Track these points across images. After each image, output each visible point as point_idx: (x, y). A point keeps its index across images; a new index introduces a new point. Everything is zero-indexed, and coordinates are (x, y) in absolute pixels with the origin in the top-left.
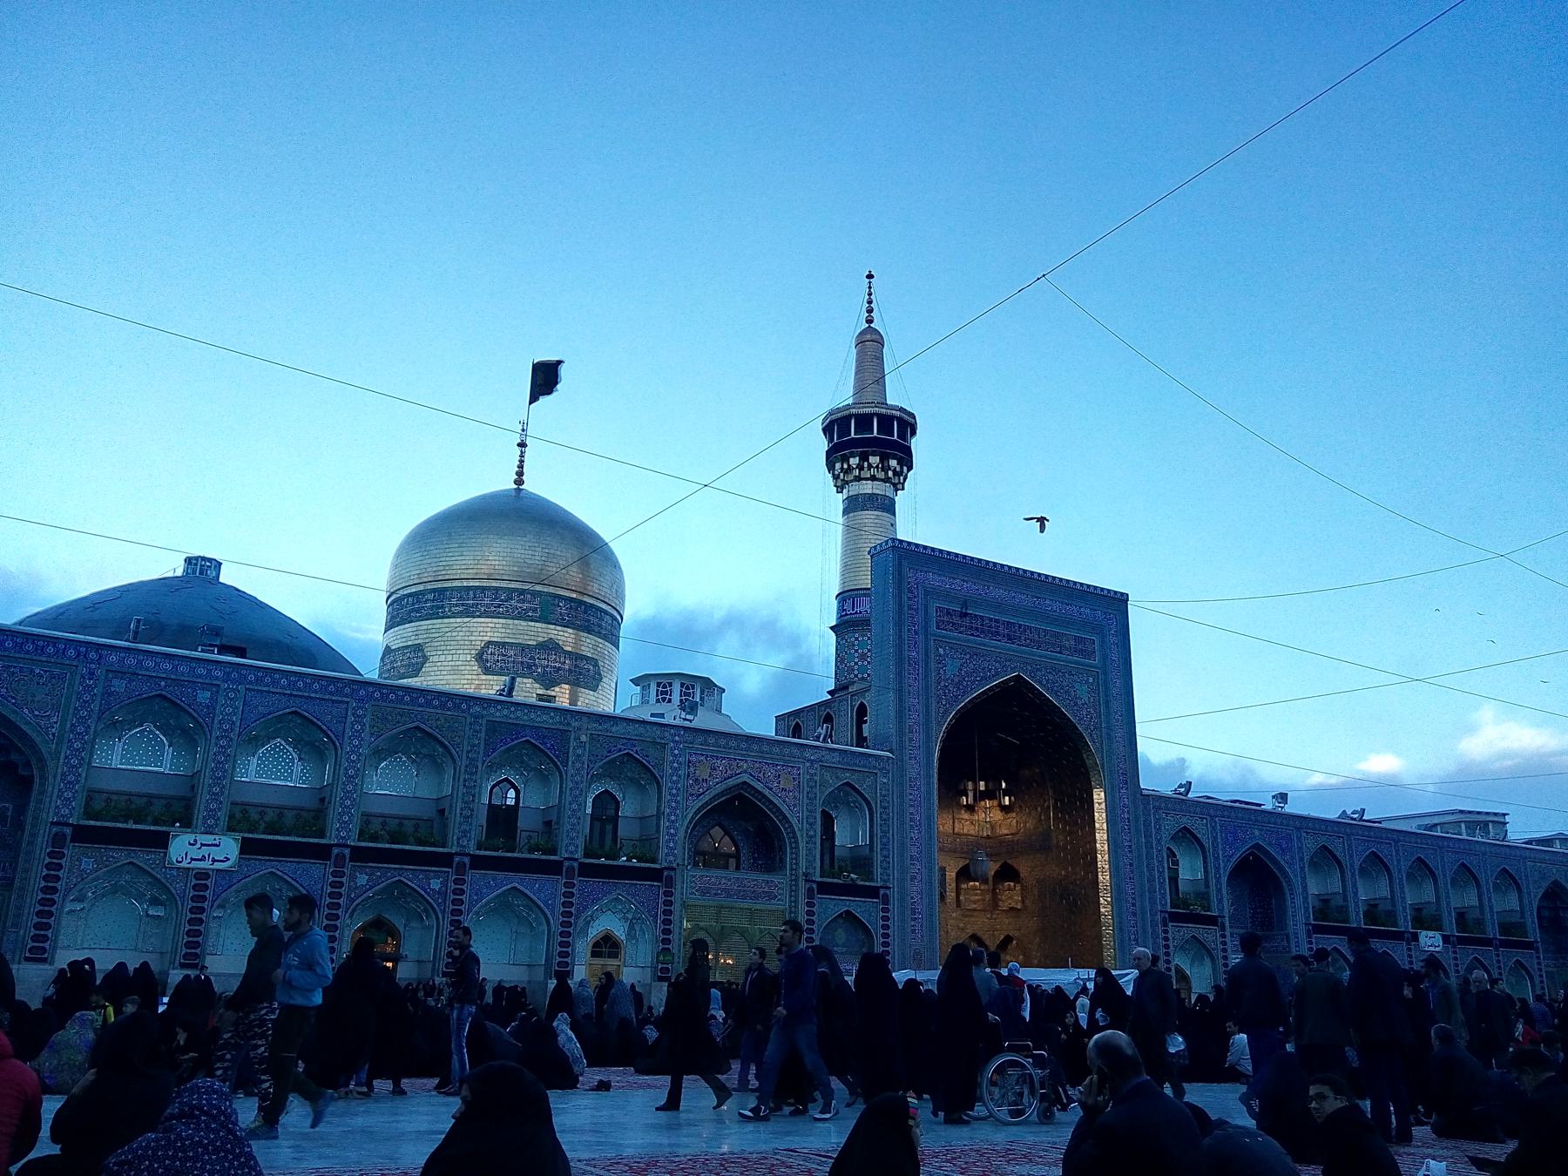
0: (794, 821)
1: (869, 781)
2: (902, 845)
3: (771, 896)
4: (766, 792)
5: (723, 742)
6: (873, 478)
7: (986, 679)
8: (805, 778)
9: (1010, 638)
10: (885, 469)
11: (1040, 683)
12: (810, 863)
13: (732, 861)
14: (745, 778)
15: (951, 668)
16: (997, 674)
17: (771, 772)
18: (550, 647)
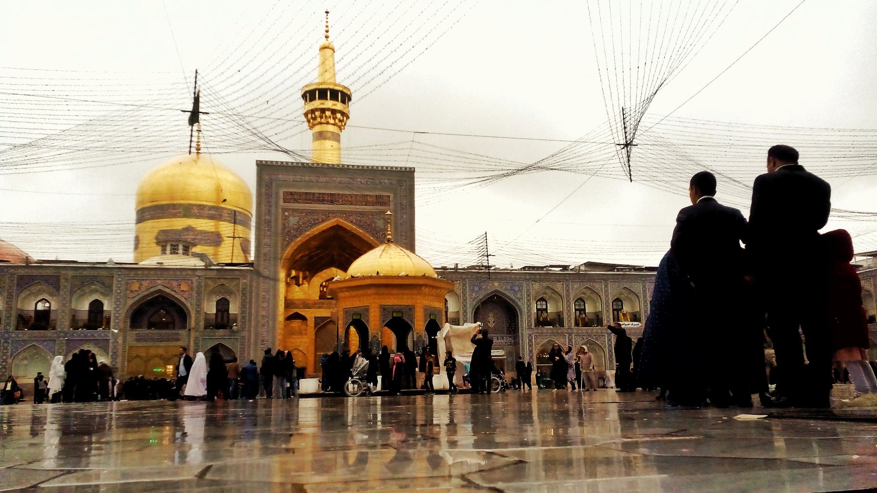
0: (189, 305)
1: (235, 283)
2: (257, 312)
3: (178, 340)
4: (173, 293)
5: (146, 272)
6: (321, 123)
7: (315, 224)
8: (195, 284)
9: (332, 202)
10: (334, 119)
11: (351, 222)
12: (197, 323)
13: (171, 325)
14: (160, 287)
15: (293, 221)
16: (323, 221)
17: (175, 284)
18: (188, 229)
